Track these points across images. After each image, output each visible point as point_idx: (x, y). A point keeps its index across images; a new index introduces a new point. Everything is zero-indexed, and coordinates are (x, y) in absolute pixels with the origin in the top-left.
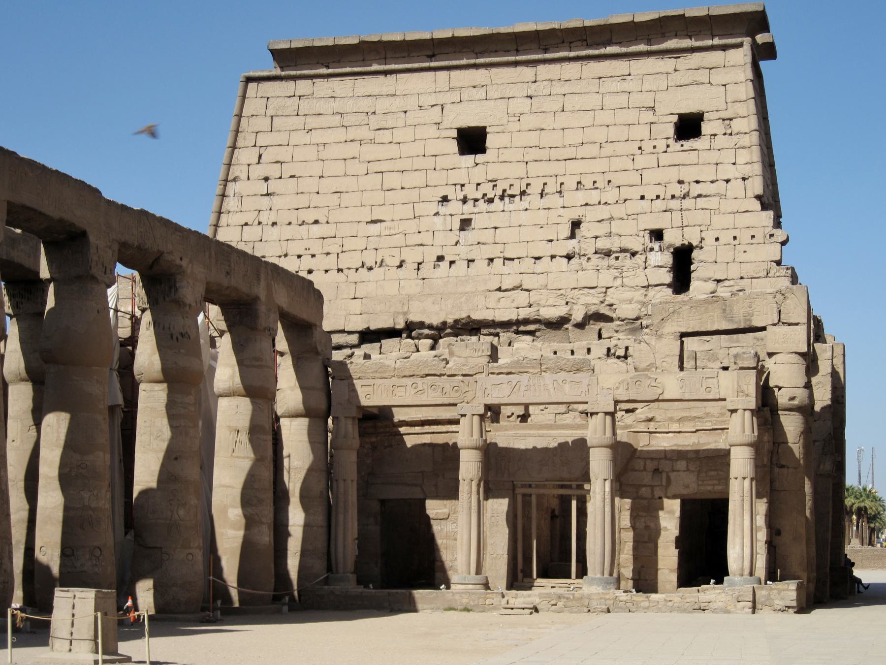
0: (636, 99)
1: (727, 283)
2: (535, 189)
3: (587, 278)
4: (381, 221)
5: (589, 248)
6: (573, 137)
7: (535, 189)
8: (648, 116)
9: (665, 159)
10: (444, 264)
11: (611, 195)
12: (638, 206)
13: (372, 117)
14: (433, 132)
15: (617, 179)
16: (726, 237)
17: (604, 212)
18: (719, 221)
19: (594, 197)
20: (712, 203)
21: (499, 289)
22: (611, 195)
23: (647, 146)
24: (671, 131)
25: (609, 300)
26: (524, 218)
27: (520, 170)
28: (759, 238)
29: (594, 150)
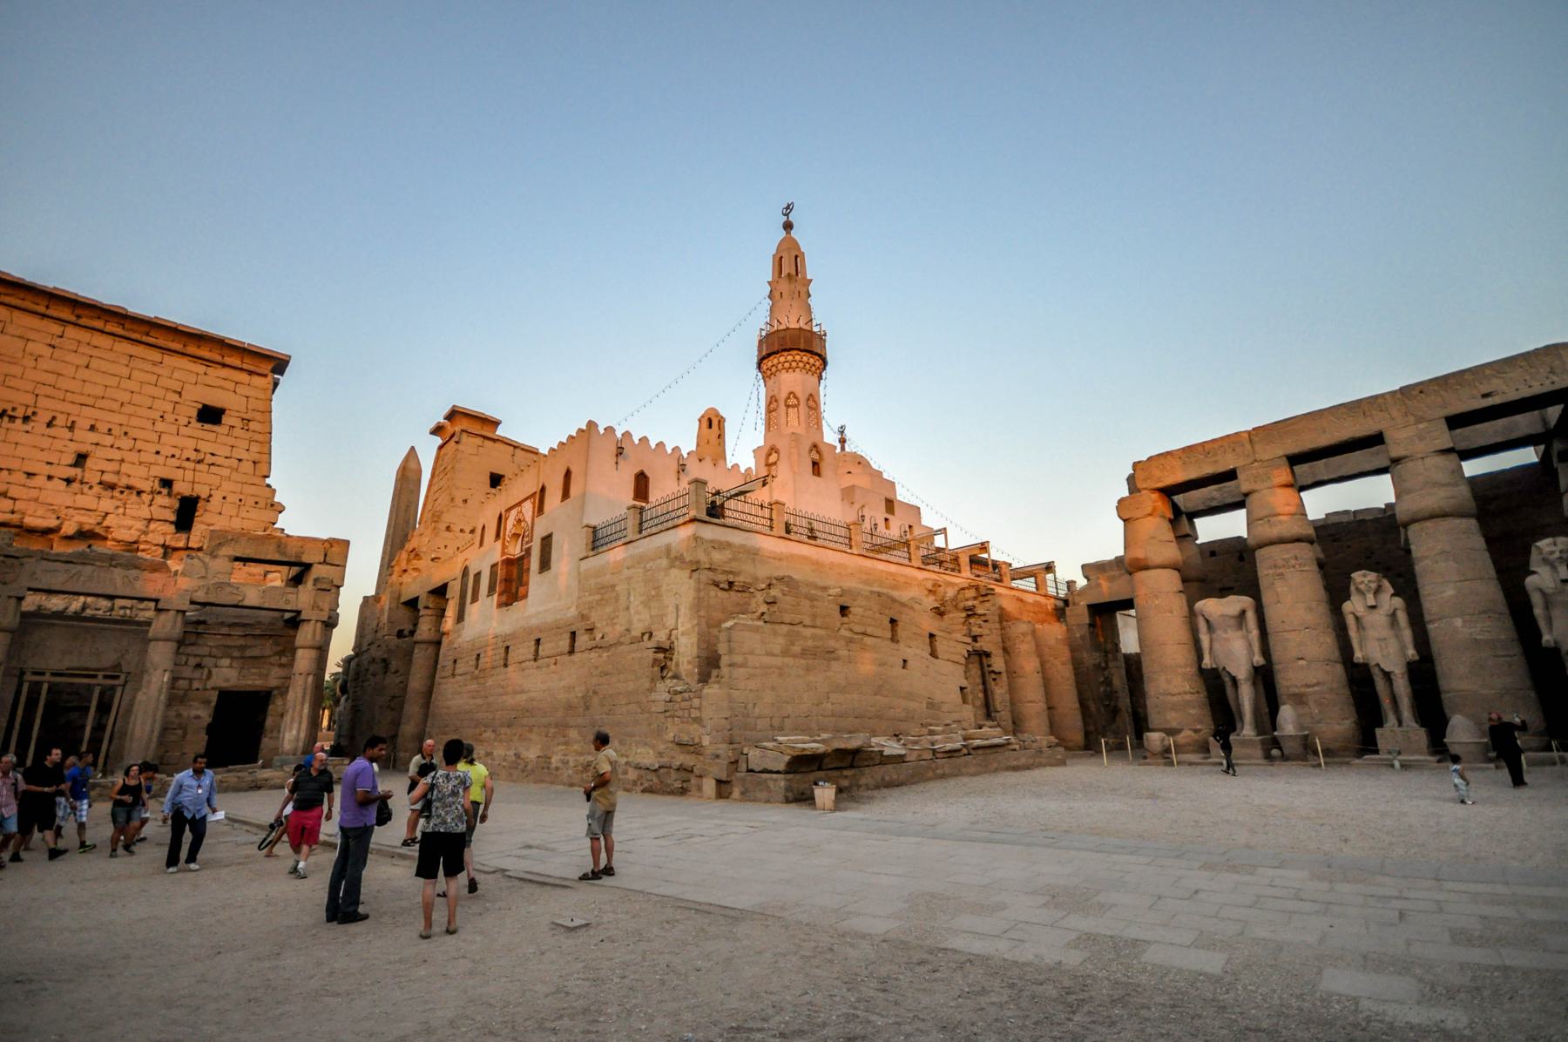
0: (163, 382)
3: (87, 500)
5: (93, 478)
6: (99, 391)
7: (45, 417)
8: (176, 398)
9: (183, 430)
15: (133, 433)
16: (231, 498)
17: (117, 455)
18: (226, 486)
19: (109, 440)
20: (226, 472)
22: (126, 443)
23: (170, 417)
24: (194, 414)
25: (106, 523)
26: (24, 438)
27: (30, 399)
28: (262, 504)
29: (116, 406)
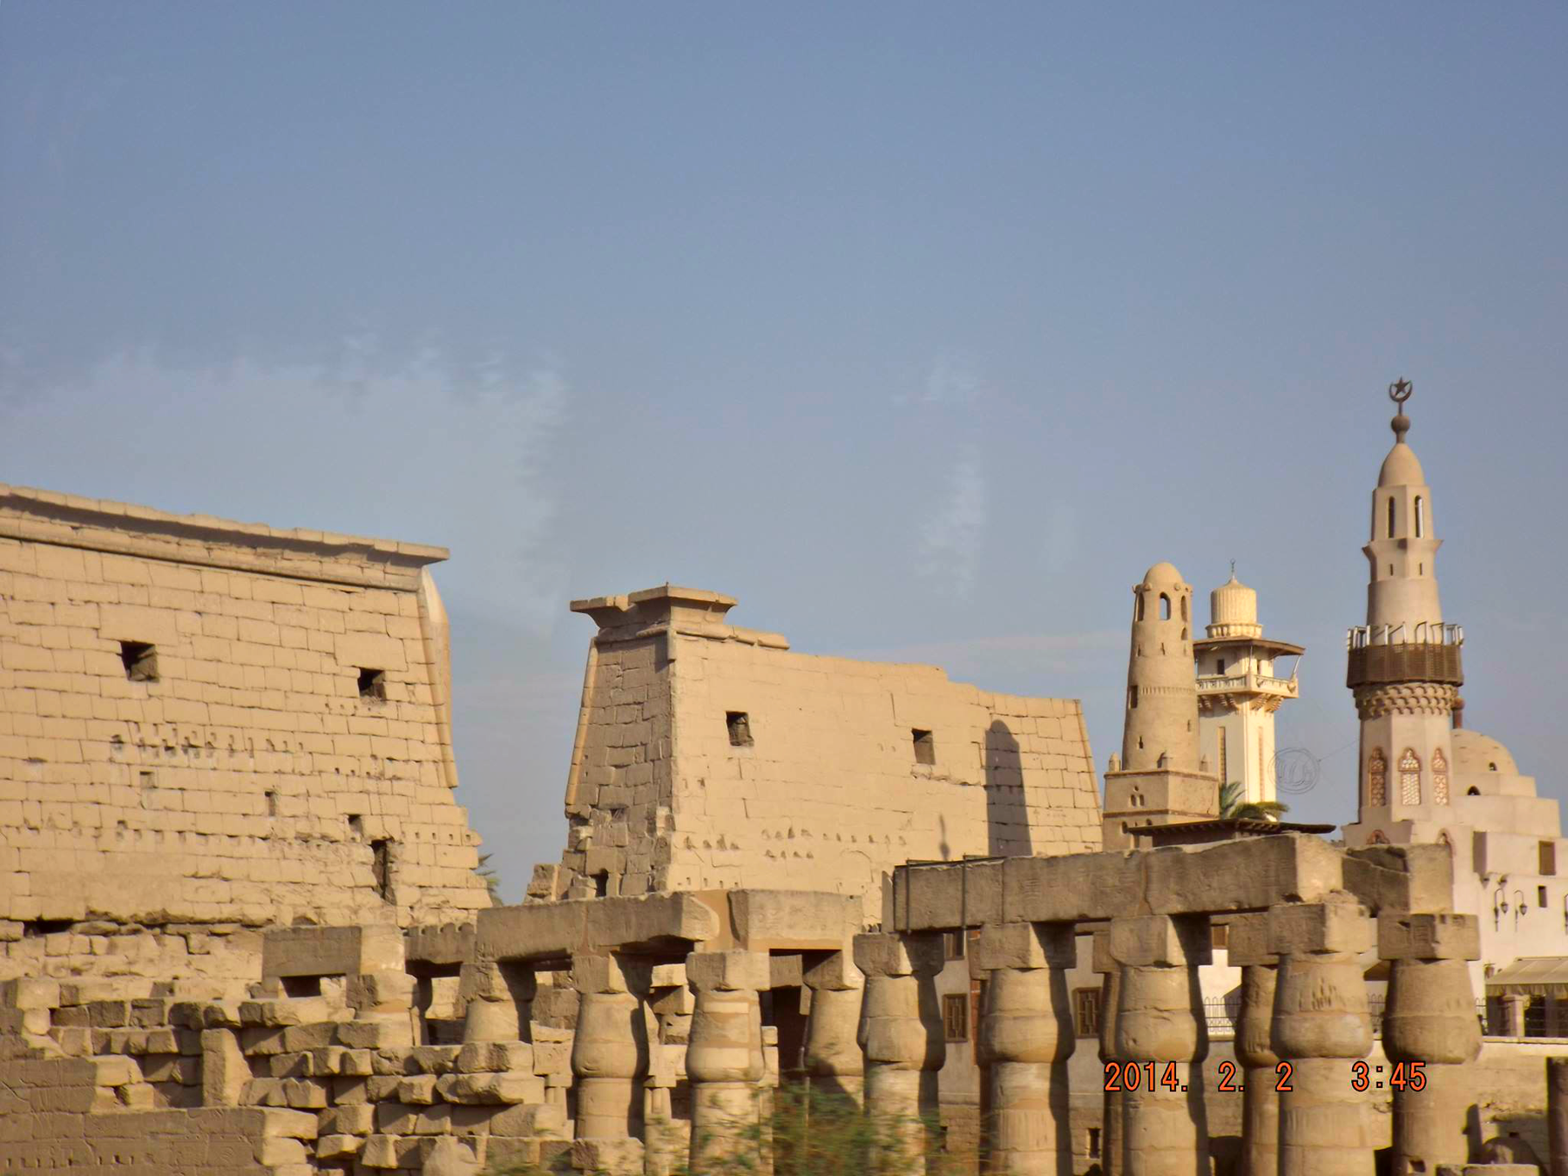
1: (432, 892)
2: (222, 743)
3: (292, 870)
4: (41, 761)
8: (329, 665)
9: (358, 725)
10: (129, 835)
11: (304, 764)
12: (332, 781)
13: (10, 603)
14: (89, 639)
16: (426, 834)
19: (286, 762)
21: (194, 876)
28: (457, 840)
